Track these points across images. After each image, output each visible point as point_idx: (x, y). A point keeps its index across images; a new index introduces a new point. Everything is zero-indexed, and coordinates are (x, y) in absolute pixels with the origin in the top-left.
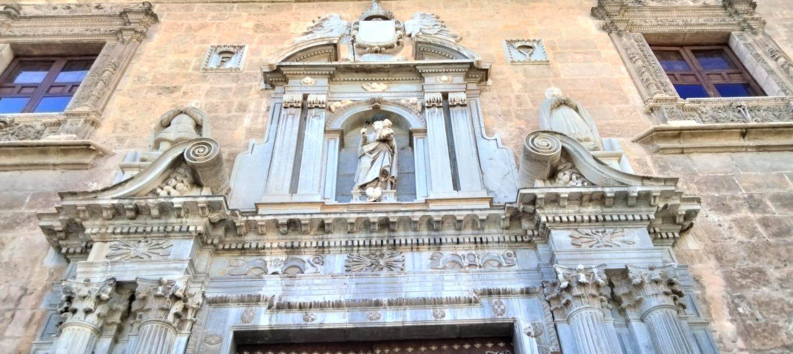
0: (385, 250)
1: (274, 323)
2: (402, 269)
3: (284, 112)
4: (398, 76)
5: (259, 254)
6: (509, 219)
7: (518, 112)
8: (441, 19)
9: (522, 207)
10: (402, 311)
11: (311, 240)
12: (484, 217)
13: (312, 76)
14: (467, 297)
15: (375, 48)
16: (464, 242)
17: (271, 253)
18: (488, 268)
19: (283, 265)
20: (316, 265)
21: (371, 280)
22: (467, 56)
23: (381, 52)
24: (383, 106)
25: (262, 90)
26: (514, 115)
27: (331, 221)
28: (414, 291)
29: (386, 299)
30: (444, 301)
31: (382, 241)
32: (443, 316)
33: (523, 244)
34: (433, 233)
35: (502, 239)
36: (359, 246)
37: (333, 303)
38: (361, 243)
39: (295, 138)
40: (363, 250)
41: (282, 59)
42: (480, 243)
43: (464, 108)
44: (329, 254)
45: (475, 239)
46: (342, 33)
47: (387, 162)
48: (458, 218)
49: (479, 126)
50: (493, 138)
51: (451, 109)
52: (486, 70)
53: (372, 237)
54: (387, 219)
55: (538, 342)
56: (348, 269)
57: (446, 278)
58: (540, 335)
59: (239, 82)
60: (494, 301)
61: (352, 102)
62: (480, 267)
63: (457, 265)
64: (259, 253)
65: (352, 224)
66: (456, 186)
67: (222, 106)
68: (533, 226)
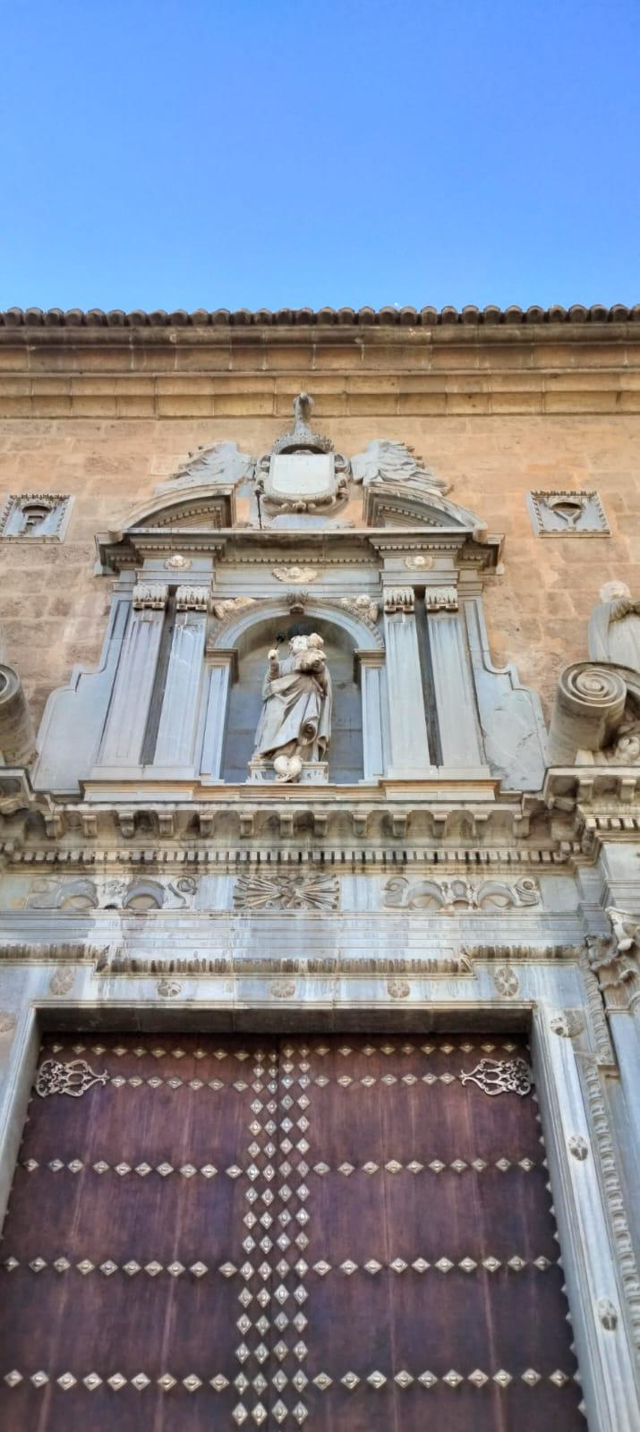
0: (305, 870)
1: (106, 996)
2: (334, 907)
3: (134, 617)
4: (337, 556)
5: (85, 873)
6: (527, 822)
7: (551, 625)
8: (417, 453)
9: (552, 799)
10: (333, 982)
11: (175, 850)
12: (484, 817)
13: (185, 553)
14: (449, 961)
15: (297, 504)
16: (447, 861)
17: (105, 870)
18: (489, 908)
19: (124, 893)
20: (183, 894)
21: (279, 924)
22: (461, 521)
23: (307, 511)
24: (309, 608)
25: (97, 576)
26: (542, 629)
27: (211, 817)
28: (356, 947)
29: (306, 960)
30: (409, 966)
31: (300, 855)
32: (406, 994)
33: (554, 867)
34: (392, 842)
35: (515, 857)
36: (259, 862)
37: (211, 962)
38: (263, 857)
39: (152, 664)
40: (267, 870)
41: (132, 523)
42: (474, 863)
43: (453, 616)
44: (205, 874)
45: (467, 855)
46: (240, 477)
47: (312, 711)
48: (437, 817)
49: (478, 649)
50: (504, 671)
51: (429, 617)
52: (495, 547)
53: (283, 847)
54: (309, 815)
55: (576, 1047)
56: (239, 902)
57: (413, 924)
58: (579, 1033)
59: (57, 562)
60: (497, 969)
61: (253, 601)
62: (475, 905)
63: (433, 901)
64: (85, 869)
65: (247, 822)
66: (435, 757)
67: (27, 604)
68: (571, 835)
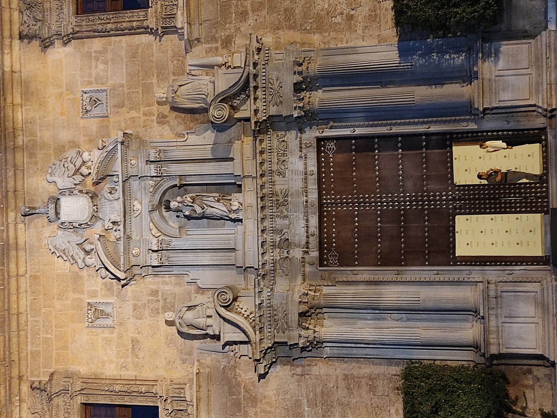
38: (271, 211)
66: (232, 159)
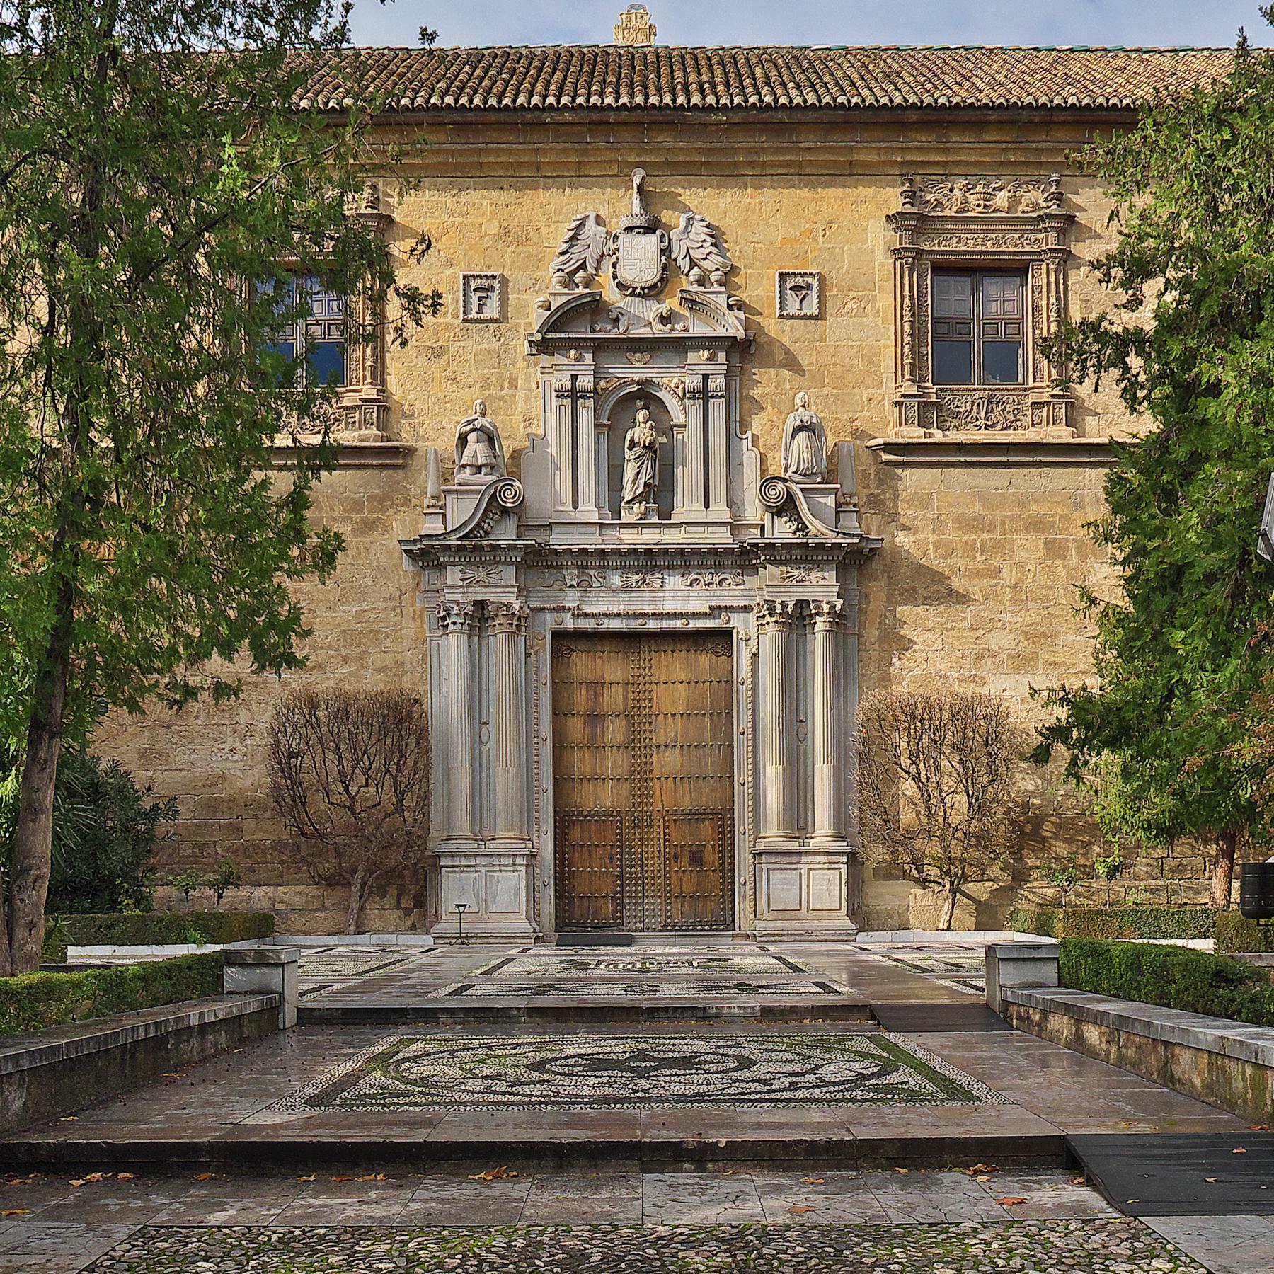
66: (707, 506)
